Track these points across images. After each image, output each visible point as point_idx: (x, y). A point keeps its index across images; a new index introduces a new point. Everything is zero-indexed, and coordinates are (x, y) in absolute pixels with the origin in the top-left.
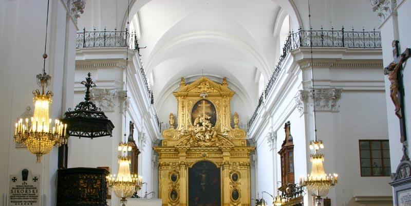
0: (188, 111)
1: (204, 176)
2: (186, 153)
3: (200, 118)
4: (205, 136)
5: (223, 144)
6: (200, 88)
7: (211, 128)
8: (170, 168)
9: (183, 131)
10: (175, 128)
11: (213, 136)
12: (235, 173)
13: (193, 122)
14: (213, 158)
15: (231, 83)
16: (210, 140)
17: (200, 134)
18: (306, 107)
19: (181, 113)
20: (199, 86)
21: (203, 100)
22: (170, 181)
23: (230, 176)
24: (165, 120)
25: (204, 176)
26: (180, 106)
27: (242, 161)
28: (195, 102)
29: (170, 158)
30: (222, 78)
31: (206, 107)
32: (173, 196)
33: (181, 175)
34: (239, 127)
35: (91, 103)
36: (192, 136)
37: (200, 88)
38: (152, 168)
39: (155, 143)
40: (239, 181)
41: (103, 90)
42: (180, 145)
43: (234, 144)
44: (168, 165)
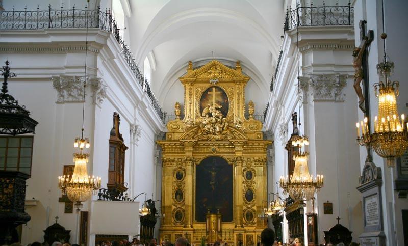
0: (197, 99)
1: (213, 173)
2: (193, 147)
3: (209, 107)
4: (215, 129)
5: (235, 138)
6: (210, 73)
7: (222, 119)
9: (189, 122)
10: (182, 119)
11: (225, 128)
12: (249, 170)
15: (245, 67)
16: (220, 133)
17: (209, 126)
18: (306, 96)
21: (214, 86)
23: (243, 174)
24: (170, 110)
25: (213, 173)
26: (188, 92)
28: (205, 89)
29: (175, 153)
30: (236, 61)
31: (217, 95)
32: (178, 196)
33: (187, 173)
34: (254, 118)
35: (8, 95)
36: (199, 128)
37: (210, 73)
38: (154, 164)
39: (158, 136)
40: (254, 179)
41: (73, 77)
42: (186, 139)
43: (247, 137)
44: (173, 161)
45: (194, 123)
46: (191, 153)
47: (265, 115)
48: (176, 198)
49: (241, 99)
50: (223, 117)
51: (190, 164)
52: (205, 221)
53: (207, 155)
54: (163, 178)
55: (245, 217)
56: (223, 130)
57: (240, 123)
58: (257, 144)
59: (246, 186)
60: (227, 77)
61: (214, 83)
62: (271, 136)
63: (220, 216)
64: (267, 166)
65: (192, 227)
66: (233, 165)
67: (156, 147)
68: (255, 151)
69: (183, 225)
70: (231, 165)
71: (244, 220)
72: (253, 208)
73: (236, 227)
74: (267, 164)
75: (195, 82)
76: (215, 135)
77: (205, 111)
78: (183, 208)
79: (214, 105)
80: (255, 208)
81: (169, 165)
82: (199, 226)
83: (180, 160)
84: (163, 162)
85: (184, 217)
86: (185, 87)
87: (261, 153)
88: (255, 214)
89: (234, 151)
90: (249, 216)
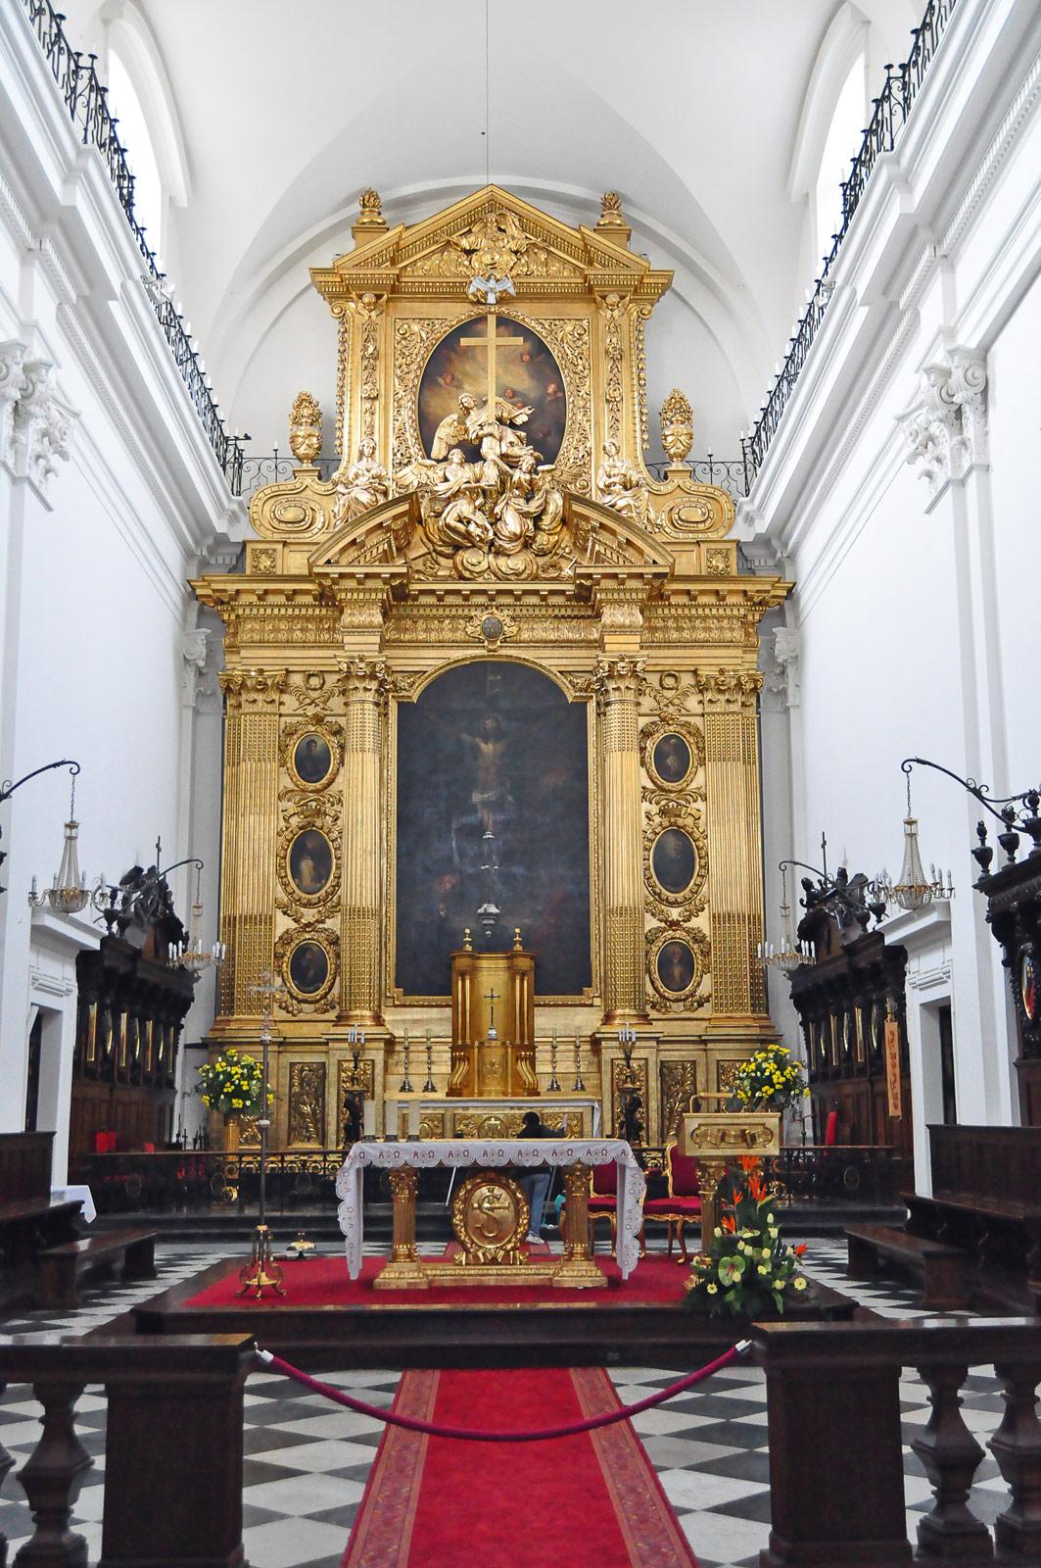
1: (487, 748)
2: (385, 615)
3: (468, 410)
4: (495, 520)
6: (469, 252)
7: (533, 471)
8: (290, 702)
9: (362, 481)
14: (549, 649)
17: (463, 507)
20: (465, 243)
23: (643, 749)
24: (268, 431)
25: (487, 748)
26: (356, 341)
27: (710, 661)
28: (442, 331)
29: (289, 644)
31: (506, 357)
32: (306, 865)
33: (349, 746)
34: (692, 473)
36: (415, 519)
38: (181, 707)
40: (698, 779)
42: (350, 564)
44: (283, 688)
45: (391, 486)
46: (377, 639)
48: (296, 872)
49: (625, 388)
50: (538, 462)
51: (370, 696)
52: (447, 989)
53: (457, 654)
54: (228, 770)
55: (654, 968)
56: (537, 528)
59: (654, 809)
60: (560, 273)
61: (491, 299)
62: (779, 566)
63: (524, 963)
65: (378, 1020)
66: (591, 707)
67: (193, 616)
68: (702, 635)
69: (332, 1015)
70: (581, 707)
72: (694, 923)
73: (608, 1018)
74: (758, 707)
75: (395, 290)
77: (444, 432)
78: (333, 924)
79: (491, 403)
80: (701, 922)
81: (260, 706)
82: (423, 1022)
83: (315, 682)
84: (228, 690)
86: (342, 317)
87: (729, 644)
88: (706, 954)
89: (596, 636)
90: (677, 964)
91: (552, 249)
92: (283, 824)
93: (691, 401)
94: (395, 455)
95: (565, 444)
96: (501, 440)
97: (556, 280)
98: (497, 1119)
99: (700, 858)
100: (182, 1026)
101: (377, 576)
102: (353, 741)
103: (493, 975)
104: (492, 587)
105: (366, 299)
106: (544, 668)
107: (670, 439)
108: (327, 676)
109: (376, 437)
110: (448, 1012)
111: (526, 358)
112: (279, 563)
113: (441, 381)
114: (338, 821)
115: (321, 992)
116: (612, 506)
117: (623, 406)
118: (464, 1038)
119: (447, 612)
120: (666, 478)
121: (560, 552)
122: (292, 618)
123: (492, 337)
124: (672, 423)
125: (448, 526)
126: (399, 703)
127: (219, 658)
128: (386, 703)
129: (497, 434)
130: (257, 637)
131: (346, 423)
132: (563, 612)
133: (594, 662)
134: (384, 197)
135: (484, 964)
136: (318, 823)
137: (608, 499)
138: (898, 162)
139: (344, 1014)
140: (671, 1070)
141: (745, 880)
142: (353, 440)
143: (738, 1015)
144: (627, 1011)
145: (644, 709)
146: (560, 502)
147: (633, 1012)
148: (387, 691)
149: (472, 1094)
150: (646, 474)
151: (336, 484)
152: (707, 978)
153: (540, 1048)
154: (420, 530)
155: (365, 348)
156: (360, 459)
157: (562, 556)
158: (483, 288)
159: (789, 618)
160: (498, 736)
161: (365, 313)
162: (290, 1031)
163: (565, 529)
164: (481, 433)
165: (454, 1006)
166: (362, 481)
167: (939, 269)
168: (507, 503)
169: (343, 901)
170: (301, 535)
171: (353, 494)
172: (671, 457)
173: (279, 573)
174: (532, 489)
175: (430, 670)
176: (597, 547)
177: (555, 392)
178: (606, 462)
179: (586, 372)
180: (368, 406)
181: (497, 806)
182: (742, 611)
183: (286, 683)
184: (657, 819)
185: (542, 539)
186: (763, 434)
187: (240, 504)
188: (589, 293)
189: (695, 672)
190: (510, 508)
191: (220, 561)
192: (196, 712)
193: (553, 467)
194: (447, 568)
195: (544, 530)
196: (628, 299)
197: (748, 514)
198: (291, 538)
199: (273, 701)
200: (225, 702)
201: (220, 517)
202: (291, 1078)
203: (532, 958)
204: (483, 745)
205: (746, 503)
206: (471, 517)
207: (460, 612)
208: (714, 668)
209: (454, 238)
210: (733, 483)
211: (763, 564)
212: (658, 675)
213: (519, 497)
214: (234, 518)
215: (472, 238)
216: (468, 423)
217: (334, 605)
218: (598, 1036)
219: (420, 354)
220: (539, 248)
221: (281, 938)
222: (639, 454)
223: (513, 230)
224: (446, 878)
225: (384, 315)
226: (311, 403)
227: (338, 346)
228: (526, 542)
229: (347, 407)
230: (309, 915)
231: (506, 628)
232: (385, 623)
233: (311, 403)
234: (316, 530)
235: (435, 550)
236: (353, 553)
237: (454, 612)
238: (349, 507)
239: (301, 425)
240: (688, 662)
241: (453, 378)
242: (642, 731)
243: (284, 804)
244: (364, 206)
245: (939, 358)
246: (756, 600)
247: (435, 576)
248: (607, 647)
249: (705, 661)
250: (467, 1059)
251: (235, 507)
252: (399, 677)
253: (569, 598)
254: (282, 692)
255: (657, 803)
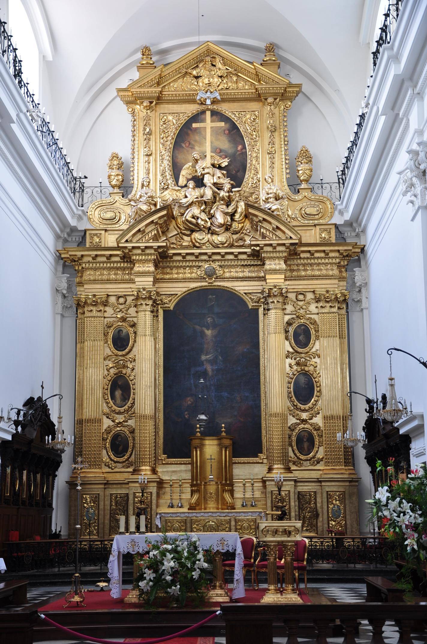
1: (209, 332)
3: (197, 161)
4: (212, 217)
5: (264, 237)
6: (197, 77)
7: (230, 191)
8: (109, 311)
9: (143, 199)
11: (237, 217)
13: (176, 178)
16: (227, 228)
17: (195, 211)
19: (142, 152)
20: (195, 73)
22: (109, 350)
24: (98, 174)
25: (209, 332)
26: (140, 125)
27: (321, 286)
28: (183, 119)
29: (109, 281)
30: (263, 45)
32: (118, 393)
34: (312, 190)
36: (171, 217)
38: (55, 314)
40: (316, 346)
42: (137, 242)
44: (105, 304)
46: (152, 279)
47: (342, 180)
48: (113, 397)
49: (277, 146)
50: (233, 186)
51: (149, 308)
54: (79, 346)
55: (294, 444)
56: (232, 220)
57: (277, 198)
58: (323, 255)
59: (293, 362)
60: (244, 87)
61: (208, 102)
62: (358, 235)
63: (227, 442)
64: (347, 312)
66: (261, 311)
67: (60, 268)
68: (317, 273)
69: (131, 470)
70: (255, 311)
71: (291, 454)
72: (315, 420)
73: (270, 470)
74: (347, 308)
75: (159, 99)
76: (213, 233)
77: (185, 173)
78: (131, 422)
79: (208, 157)
80: (318, 420)
81: (94, 313)
82: (176, 471)
83: (122, 300)
84: (78, 305)
85: (134, 447)
86: (133, 113)
89: (262, 274)
90: (305, 442)
91: (239, 74)
92: (106, 372)
93: (312, 151)
94: (160, 184)
95: (246, 176)
96: (213, 176)
97: (242, 91)
98: (213, 522)
99: (317, 387)
100: (56, 476)
101: (151, 247)
102: (140, 329)
103: (211, 448)
104: (209, 251)
105: (145, 104)
106: (237, 291)
107: (300, 172)
108: (128, 298)
109: (151, 175)
110: (190, 466)
111: (227, 132)
112: (103, 240)
113: (184, 145)
114: (134, 371)
115: (126, 457)
116: (269, 209)
117: (276, 156)
118: (197, 481)
119: (188, 264)
120: (299, 192)
121: (244, 232)
122: (110, 269)
123: (208, 124)
124: (302, 163)
125: (187, 220)
126: (164, 311)
127: (74, 288)
128: (157, 311)
129: (211, 172)
130: (92, 278)
131: (136, 168)
132: (246, 263)
133: (261, 288)
134: (153, 49)
135: (207, 442)
136: (124, 372)
137: (267, 205)
138: (392, 48)
139: (137, 468)
140: (303, 496)
141: (340, 399)
142: (140, 177)
143: (338, 467)
144: (279, 466)
145: (287, 311)
146: (244, 207)
147: (282, 466)
148: (158, 304)
149: (201, 509)
150: (288, 190)
151: (130, 201)
152: (321, 449)
153: (236, 485)
154: (174, 222)
155: (145, 129)
156: (142, 187)
157: (246, 234)
158: (205, 96)
159: (363, 263)
160: (214, 326)
161: (145, 111)
162: (111, 477)
163: (247, 220)
164: (203, 172)
165: (192, 464)
166: (143, 199)
167: (416, 99)
168: (217, 208)
169: (136, 411)
170: (114, 226)
171: (139, 206)
172: (301, 181)
173: (103, 246)
174: (230, 201)
175: (179, 293)
176: (262, 230)
177: (242, 149)
178: (267, 186)
179: (258, 138)
180: (147, 159)
181: (213, 362)
182: (338, 260)
183: (107, 301)
184: (295, 367)
185: (236, 226)
186: (346, 169)
187: (83, 211)
188: (259, 97)
189: (314, 292)
190: (219, 211)
191: (74, 239)
192: (62, 316)
193: (240, 189)
194: (188, 241)
195: (236, 221)
196: (278, 100)
197: (340, 210)
198: (109, 227)
199: (100, 311)
200: (77, 311)
201: (73, 217)
202: (111, 501)
203: (231, 439)
204: (206, 331)
205: (339, 205)
206: (199, 215)
207: (194, 264)
208: (323, 290)
209: (189, 71)
210: (333, 194)
211: (349, 235)
212: (295, 293)
213: (223, 204)
214: (80, 218)
215: (198, 70)
216: (197, 168)
217: (131, 262)
218: (264, 479)
219: (173, 132)
220: (233, 74)
221: (106, 430)
222: (285, 180)
223: (219, 65)
224: (189, 399)
225: (154, 112)
226: (118, 158)
227: (131, 128)
228: (227, 227)
229: (136, 160)
230: (120, 418)
231: (217, 272)
232: (156, 270)
233: (118, 158)
234: (121, 223)
235: (181, 233)
236: (139, 236)
237: (191, 264)
238: (137, 213)
239: (113, 169)
240: (310, 287)
241: (190, 144)
242: (287, 323)
243: (107, 362)
244: (143, 55)
245: (415, 147)
246: (345, 254)
247: (181, 245)
248: (268, 281)
249: (319, 286)
250: (198, 491)
251: (80, 213)
252: (164, 297)
253: (249, 256)
254: (105, 305)
255: (295, 359)
